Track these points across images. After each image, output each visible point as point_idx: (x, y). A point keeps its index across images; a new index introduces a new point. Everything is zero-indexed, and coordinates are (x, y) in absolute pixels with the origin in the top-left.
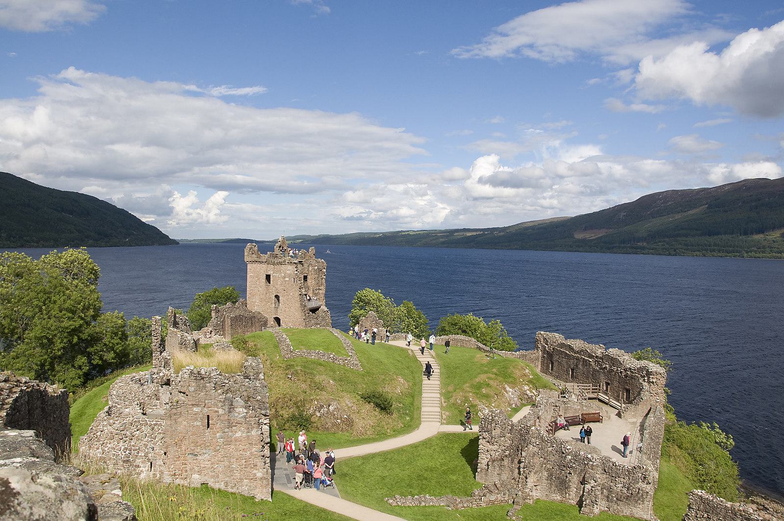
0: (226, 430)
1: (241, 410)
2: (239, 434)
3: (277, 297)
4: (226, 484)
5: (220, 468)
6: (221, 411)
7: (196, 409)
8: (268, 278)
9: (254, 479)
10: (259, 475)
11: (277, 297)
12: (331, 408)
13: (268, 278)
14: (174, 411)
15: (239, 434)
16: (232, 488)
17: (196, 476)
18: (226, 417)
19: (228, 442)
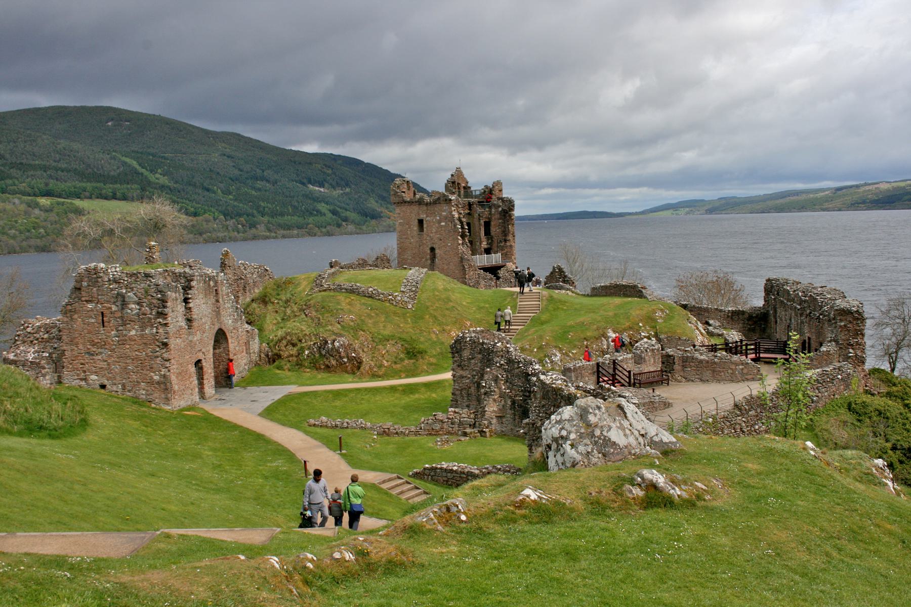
0: (121, 328)
1: (133, 306)
2: (133, 333)
3: (432, 249)
4: (124, 386)
5: (116, 368)
6: (114, 308)
7: (90, 306)
8: (421, 222)
9: (151, 382)
10: (156, 378)
11: (432, 249)
12: (337, 344)
13: (421, 222)
14: (69, 307)
15: (133, 333)
16: (129, 391)
17: (94, 377)
18: (119, 314)
19: (122, 343)
